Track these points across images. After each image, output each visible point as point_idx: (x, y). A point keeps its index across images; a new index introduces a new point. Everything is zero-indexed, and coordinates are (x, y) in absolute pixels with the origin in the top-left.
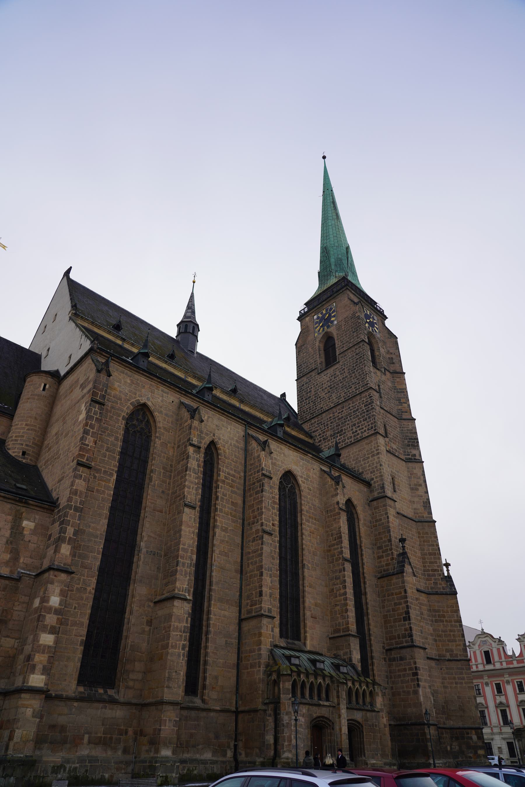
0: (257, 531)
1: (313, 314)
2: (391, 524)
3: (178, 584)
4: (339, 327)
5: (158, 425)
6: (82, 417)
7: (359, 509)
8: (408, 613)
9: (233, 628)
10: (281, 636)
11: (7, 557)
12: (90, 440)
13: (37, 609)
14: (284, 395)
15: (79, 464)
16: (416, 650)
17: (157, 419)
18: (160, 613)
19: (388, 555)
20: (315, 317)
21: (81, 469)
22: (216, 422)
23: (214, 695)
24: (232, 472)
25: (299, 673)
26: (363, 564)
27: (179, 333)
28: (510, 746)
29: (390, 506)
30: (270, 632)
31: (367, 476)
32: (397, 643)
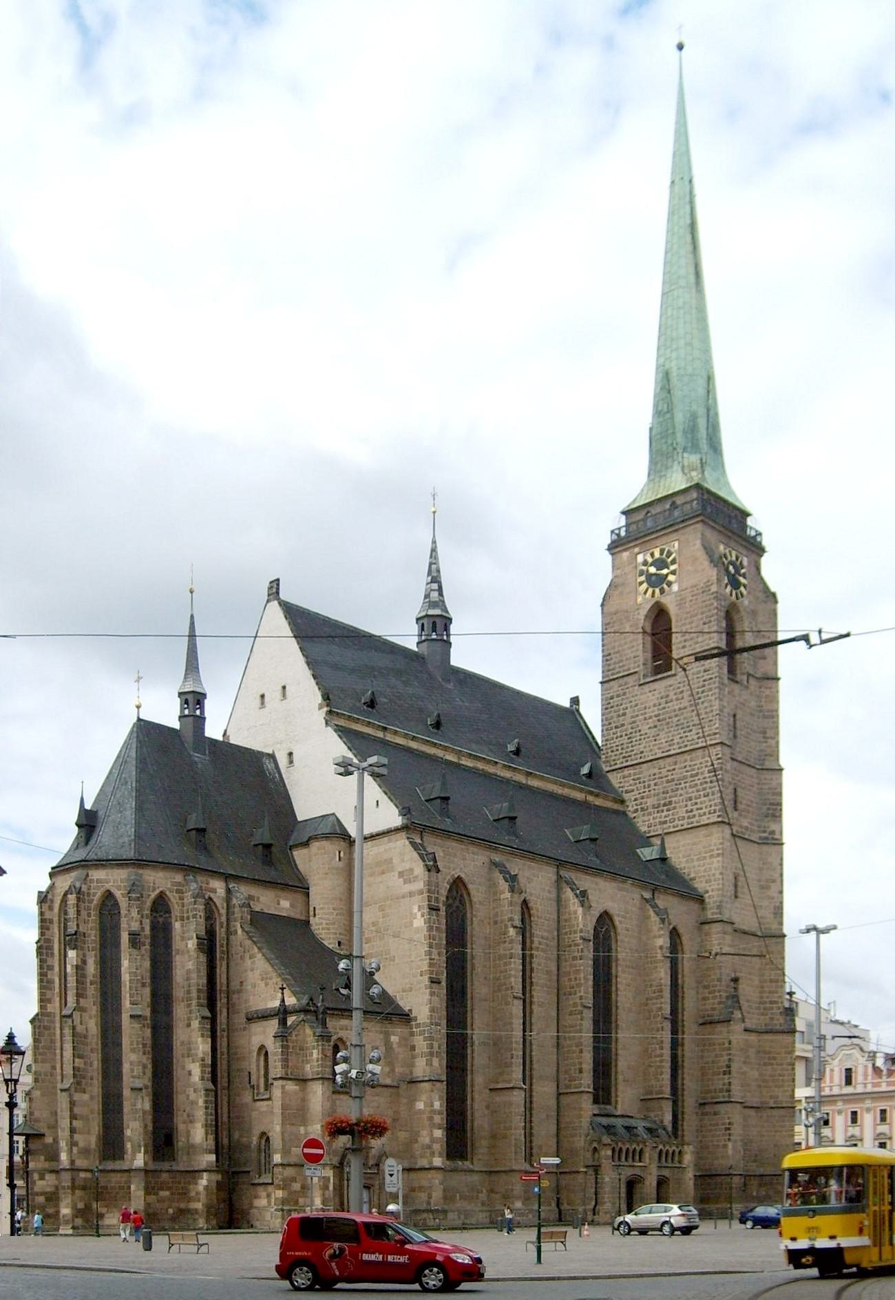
1: (637, 550)
5: (475, 900)
6: (419, 922)
17: (473, 893)
18: (498, 1099)
20: (640, 558)
22: (527, 874)
24: (546, 934)
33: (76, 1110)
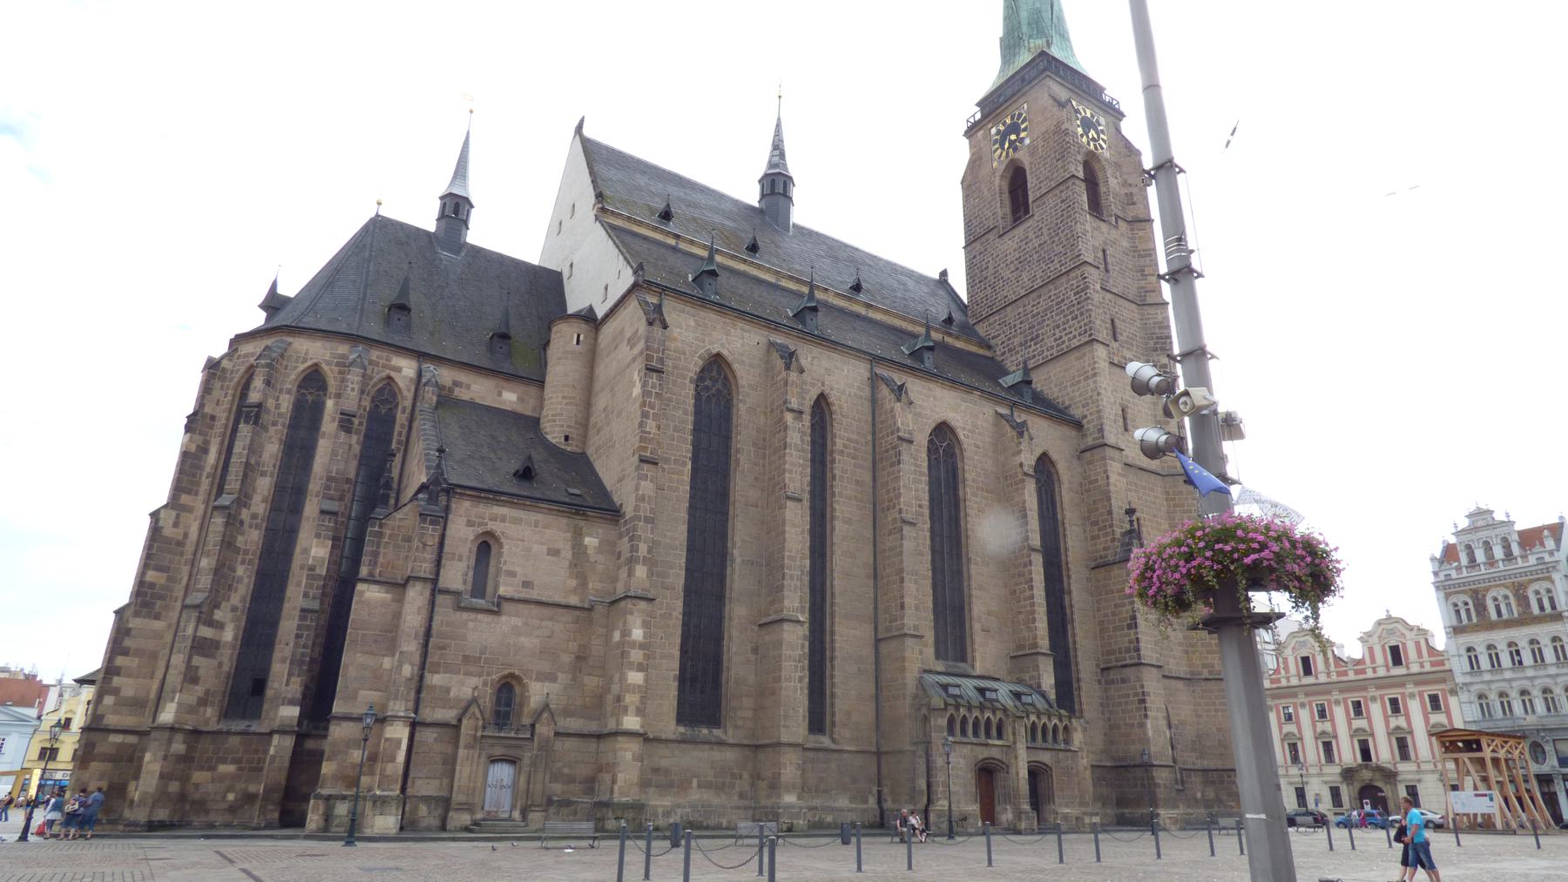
0: (894, 520)
2: (1112, 488)
3: (786, 603)
4: (1033, 150)
7: (1062, 467)
8: (1134, 618)
9: (868, 652)
10: (938, 656)
11: (573, 583)
12: (651, 425)
13: (618, 644)
14: (944, 274)
15: (643, 460)
16: (1144, 669)
17: (739, 374)
18: (767, 638)
19: (1107, 534)
20: (994, 131)
21: (646, 466)
23: (847, 733)
24: (855, 437)
25: (957, 707)
26: (1066, 550)
27: (763, 196)
28: (1335, 793)
29: (1112, 459)
30: (919, 656)
31: (1077, 412)
32: (1117, 660)
33: (127, 643)
